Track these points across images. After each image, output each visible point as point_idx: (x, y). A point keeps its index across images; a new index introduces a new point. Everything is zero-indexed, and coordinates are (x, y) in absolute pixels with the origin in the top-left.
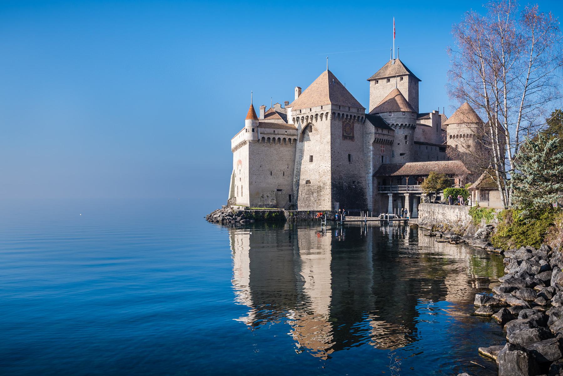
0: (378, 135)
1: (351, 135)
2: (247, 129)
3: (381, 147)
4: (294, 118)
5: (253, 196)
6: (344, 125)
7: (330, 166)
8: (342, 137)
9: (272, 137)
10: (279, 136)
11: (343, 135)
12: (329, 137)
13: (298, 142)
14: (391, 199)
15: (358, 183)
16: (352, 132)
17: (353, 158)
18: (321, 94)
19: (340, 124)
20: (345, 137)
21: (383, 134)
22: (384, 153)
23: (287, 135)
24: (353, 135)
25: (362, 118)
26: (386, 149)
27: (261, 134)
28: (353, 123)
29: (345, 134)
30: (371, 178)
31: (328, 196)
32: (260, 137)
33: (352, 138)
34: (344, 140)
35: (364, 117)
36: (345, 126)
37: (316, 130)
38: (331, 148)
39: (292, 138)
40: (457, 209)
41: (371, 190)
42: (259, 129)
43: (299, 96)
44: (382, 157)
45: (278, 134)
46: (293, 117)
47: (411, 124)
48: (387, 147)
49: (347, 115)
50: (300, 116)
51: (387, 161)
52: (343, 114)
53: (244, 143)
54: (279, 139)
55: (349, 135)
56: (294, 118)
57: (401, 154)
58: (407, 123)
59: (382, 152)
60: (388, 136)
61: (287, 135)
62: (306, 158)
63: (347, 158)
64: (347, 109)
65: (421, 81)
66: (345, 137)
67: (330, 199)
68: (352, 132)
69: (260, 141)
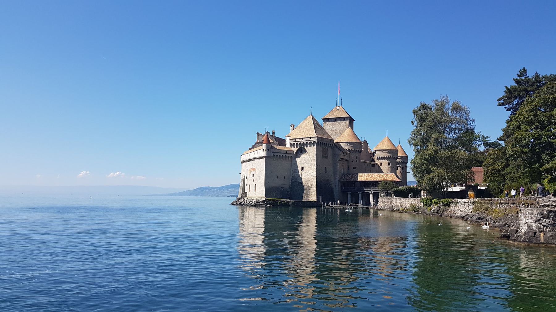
1: (326, 156)
2: (264, 150)
4: (291, 144)
5: (268, 191)
7: (316, 174)
9: (278, 154)
10: (283, 154)
12: (315, 156)
13: (293, 158)
14: (349, 195)
15: (330, 185)
17: (327, 169)
18: (309, 130)
19: (320, 148)
20: (323, 157)
22: (344, 167)
23: (288, 154)
25: (332, 145)
27: (273, 152)
28: (328, 148)
30: (337, 182)
31: (314, 192)
32: (272, 154)
33: (327, 157)
34: (322, 158)
35: (333, 145)
37: (306, 151)
38: (316, 163)
39: (290, 156)
40: (411, 200)
41: (337, 189)
42: (272, 149)
43: (293, 130)
44: (343, 169)
45: (282, 153)
46: (290, 143)
49: (325, 143)
50: (296, 143)
51: (346, 171)
52: (323, 143)
53: (261, 158)
54: (283, 156)
56: (291, 144)
57: (354, 168)
61: (288, 154)
62: (300, 169)
63: (324, 169)
65: (355, 121)
66: (323, 157)
67: (316, 194)
69: (272, 157)
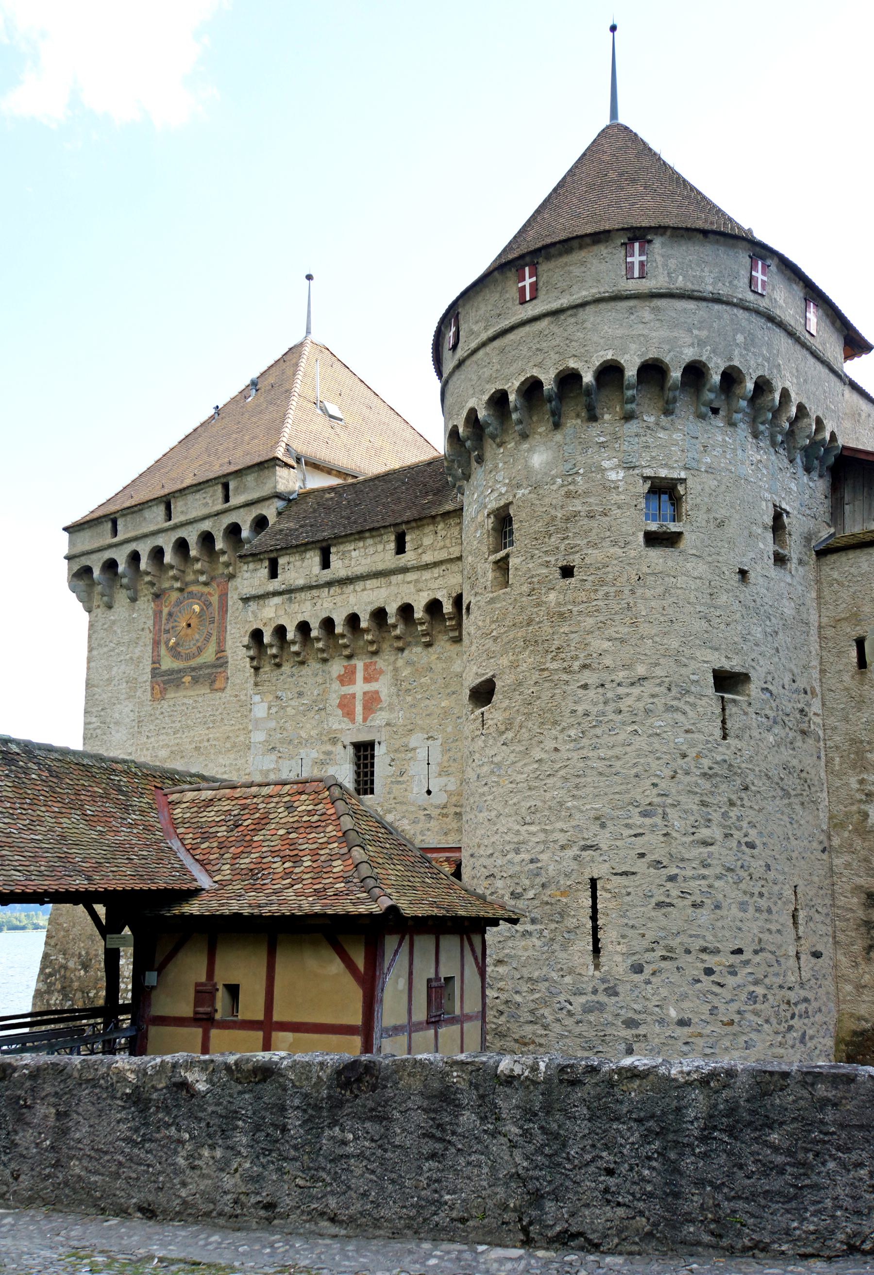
0: (277, 600)
1: (209, 655)
3: (347, 678)
6: (165, 611)
8: (148, 683)
11: (155, 673)
16: (214, 638)
21: (329, 584)
22: (380, 718)
24: (221, 650)
26: (397, 681)
29: (168, 663)
36: (170, 614)
47: (513, 386)
48: (408, 663)
55: (193, 663)
58: (471, 403)
59: (350, 714)
60: (394, 579)
64: (155, 518)
68: (214, 638)
